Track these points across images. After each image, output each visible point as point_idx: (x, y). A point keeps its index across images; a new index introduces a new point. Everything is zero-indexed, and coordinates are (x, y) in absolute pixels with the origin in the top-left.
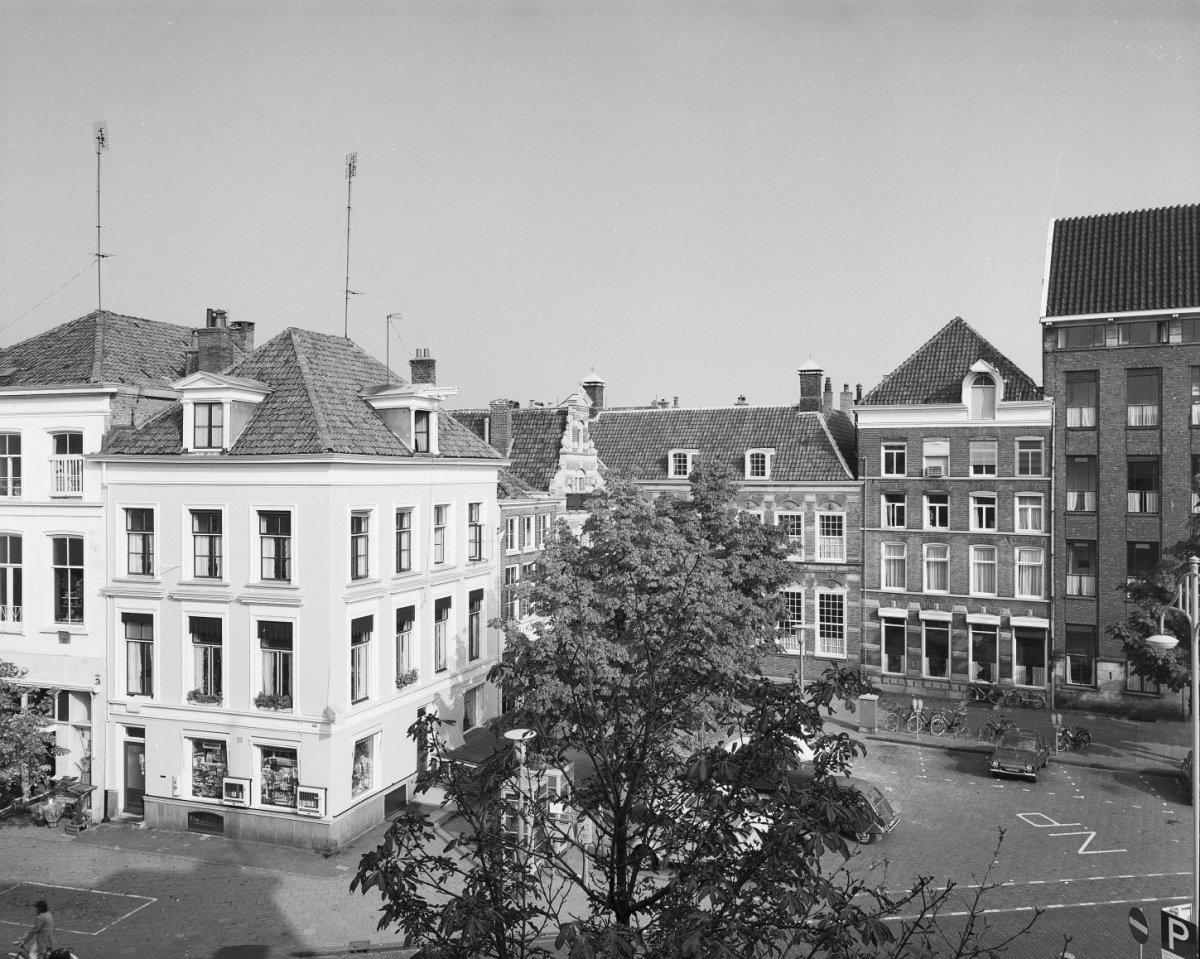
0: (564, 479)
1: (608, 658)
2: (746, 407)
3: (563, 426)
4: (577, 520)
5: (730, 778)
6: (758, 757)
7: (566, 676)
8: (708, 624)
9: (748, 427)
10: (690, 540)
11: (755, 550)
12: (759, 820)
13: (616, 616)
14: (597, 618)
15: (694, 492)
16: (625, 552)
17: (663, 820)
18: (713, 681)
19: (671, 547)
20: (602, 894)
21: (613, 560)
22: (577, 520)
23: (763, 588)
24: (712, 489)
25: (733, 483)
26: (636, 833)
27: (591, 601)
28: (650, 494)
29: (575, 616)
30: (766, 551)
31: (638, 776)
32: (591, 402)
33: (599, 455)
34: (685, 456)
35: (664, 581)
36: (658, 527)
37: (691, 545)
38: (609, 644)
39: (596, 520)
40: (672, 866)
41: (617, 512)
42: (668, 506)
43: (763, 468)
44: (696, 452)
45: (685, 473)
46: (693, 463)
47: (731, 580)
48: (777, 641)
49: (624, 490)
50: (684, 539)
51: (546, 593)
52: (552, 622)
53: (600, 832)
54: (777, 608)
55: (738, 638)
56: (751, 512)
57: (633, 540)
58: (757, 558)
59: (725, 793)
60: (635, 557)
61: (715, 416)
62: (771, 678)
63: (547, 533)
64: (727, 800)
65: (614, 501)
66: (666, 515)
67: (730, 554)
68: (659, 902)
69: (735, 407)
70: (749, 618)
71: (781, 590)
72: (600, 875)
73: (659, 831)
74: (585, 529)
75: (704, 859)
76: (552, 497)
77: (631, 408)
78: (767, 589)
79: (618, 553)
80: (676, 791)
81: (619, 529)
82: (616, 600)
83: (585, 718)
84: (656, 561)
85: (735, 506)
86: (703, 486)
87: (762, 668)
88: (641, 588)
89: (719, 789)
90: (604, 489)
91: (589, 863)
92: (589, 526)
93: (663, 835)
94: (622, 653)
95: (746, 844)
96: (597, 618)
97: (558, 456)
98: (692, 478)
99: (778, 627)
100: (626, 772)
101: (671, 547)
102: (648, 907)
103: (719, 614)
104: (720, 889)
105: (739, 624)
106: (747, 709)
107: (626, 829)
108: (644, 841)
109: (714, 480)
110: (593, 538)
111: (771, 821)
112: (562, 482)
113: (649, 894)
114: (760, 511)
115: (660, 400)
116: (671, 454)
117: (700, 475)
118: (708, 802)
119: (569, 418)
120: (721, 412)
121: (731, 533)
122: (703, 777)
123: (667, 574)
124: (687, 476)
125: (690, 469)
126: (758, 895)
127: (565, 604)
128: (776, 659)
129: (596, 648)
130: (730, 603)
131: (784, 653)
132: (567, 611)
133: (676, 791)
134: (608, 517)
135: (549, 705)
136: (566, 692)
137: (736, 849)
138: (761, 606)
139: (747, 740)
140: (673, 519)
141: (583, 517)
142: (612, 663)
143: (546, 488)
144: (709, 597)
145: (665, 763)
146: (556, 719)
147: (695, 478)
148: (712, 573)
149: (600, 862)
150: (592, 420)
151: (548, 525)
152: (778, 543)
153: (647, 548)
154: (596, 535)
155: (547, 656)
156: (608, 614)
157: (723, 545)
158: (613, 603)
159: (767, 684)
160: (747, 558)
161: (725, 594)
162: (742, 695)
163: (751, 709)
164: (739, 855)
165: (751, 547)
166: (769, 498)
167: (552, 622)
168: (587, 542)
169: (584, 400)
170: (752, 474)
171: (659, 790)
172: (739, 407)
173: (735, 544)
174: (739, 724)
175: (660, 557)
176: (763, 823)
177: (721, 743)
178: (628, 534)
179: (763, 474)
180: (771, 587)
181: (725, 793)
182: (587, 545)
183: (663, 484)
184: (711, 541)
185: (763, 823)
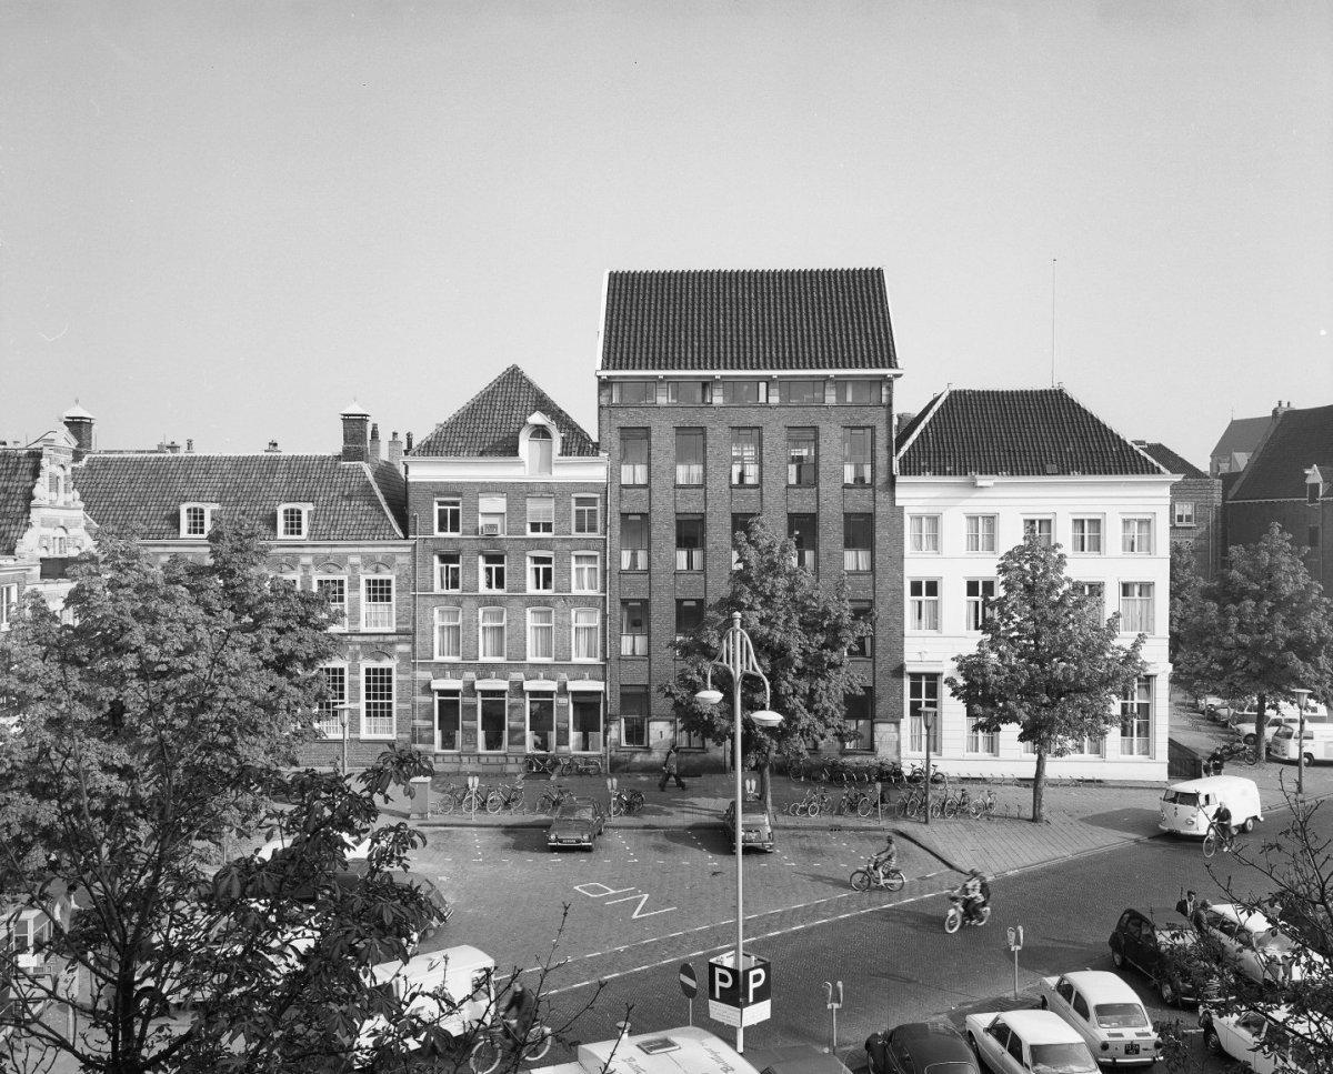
0: (36, 538)
1: (101, 763)
2: (278, 454)
3: (36, 472)
4: (56, 593)
5: (270, 890)
6: (303, 860)
7: (40, 792)
8: (234, 711)
9: (280, 478)
10: (209, 612)
11: (290, 622)
12: (304, 934)
13: (111, 710)
14: (83, 713)
15: (214, 554)
16: (123, 629)
17: (181, 953)
18: (244, 777)
19: (185, 621)
20: (100, 1059)
21: (106, 640)
22: (56, 593)
23: (299, 664)
24: (237, 550)
25: (261, 543)
26: (145, 976)
27: (77, 693)
28: (157, 557)
29: (54, 714)
30: (303, 622)
31: (148, 903)
32: (74, 443)
33: (87, 509)
34: (202, 511)
35: (177, 663)
36: (168, 598)
37: (211, 618)
38: (102, 745)
39: (83, 590)
40: (195, 1006)
41: (112, 580)
42: (180, 571)
43: (299, 525)
44: (217, 506)
45: (202, 532)
46: (213, 519)
47: (261, 658)
48: (316, 725)
49: (122, 553)
50: (201, 611)
51: (12, 687)
52: (20, 723)
53: (101, 981)
54: (316, 686)
55: (270, 726)
56: (285, 577)
57: (135, 614)
58: (292, 630)
59: (262, 909)
60: (137, 635)
61: (240, 463)
62: (318, 769)
63: (13, 609)
64: (264, 916)
65: (109, 566)
66: (178, 582)
67: (259, 627)
68: (177, 1053)
69: (265, 454)
70: (283, 701)
71: (321, 666)
72: (101, 1034)
73: (177, 967)
74: (68, 602)
75: (236, 992)
76: (20, 562)
77: (129, 452)
78: (305, 665)
79: (114, 630)
80: (199, 915)
81: (115, 601)
82: (112, 690)
83: (76, 841)
84: (165, 638)
85: (265, 570)
86: (225, 547)
87: (299, 758)
88: (146, 672)
89: (253, 905)
90: (94, 551)
91: (84, 1024)
92: (73, 599)
93: (184, 970)
94: (120, 754)
95: (287, 965)
96: (83, 713)
97: (28, 510)
98: (210, 538)
99: (317, 710)
100: (134, 900)
101: (185, 621)
102: (163, 1063)
103: (247, 698)
104: (256, 1023)
105: (270, 709)
106: (288, 808)
107: (135, 970)
108: (157, 983)
109: (240, 540)
110: (78, 614)
111: (318, 934)
112: (33, 543)
113: (164, 1046)
114: (295, 576)
115: (168, 443)
116: (183, 508)
117: (222, 533)
118: (243, 921)
119: (44, 462)
120: (246, 459)
121: (261, 602)
122: (235, 894)
123: (180, 653)
124: (205, 535)
125: (208, 526)
126: (301, 1022)
127: (40, 699)
128: (314, 746)
129: (83, 751)
130: (258, 684)
131: (324, 738)
132: (41, 708)
133: (199, 915)
134: (99, 587)
135: (17, 830)
136: (47, 812)
137: (274, 973)
138: (297, 686)
139: (288, 842)
140: (188, 587)
141: (65, 587)
142: (107, 769)
143: (10, 551)
144: (233, 679)
145: (183, 881)
146: (28, 847)
147: (215, 538)
148: (237, 650)
149: (97, 1018)
150: (76, 465)
151: (14, 598)
152: (317, 613)
153: (154, 622)
154: (84, 609)
155: (14, 767)
156: (100, 708)
157: (250, 616)
158: (107, 694)
159: (313, 775)
160: (281, 631)
161: (254, 675)
162: (282, 790)
163: (293, 807)
164: (278, 980)
165: (285, 618)
166: (307, 560)
167: (20, 723)
168: (70, 618)
169: (65, 440)
170: (286, 532)
171: (177, 917)
172: (269, 454)
173: (266, 615)
174: (280, 826)
175: (170, 634)
176: (309, 937)
177: (257, 850)
178: (128, 606)
179: (299, 533)
180: (309, 663)
181: (262, 909)
182: (71, 623)
183: (173, 545)
184: (236, 612)
185: (309, 937)
